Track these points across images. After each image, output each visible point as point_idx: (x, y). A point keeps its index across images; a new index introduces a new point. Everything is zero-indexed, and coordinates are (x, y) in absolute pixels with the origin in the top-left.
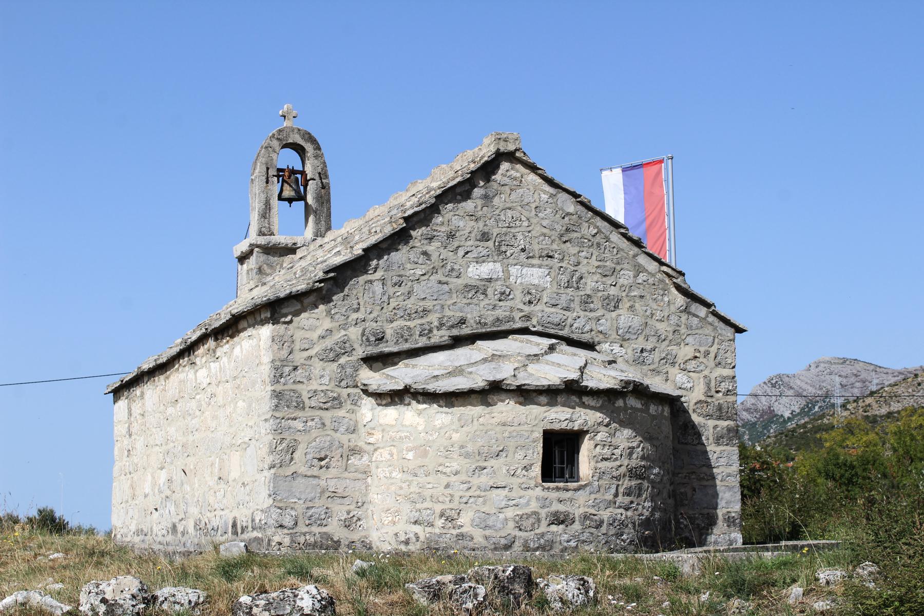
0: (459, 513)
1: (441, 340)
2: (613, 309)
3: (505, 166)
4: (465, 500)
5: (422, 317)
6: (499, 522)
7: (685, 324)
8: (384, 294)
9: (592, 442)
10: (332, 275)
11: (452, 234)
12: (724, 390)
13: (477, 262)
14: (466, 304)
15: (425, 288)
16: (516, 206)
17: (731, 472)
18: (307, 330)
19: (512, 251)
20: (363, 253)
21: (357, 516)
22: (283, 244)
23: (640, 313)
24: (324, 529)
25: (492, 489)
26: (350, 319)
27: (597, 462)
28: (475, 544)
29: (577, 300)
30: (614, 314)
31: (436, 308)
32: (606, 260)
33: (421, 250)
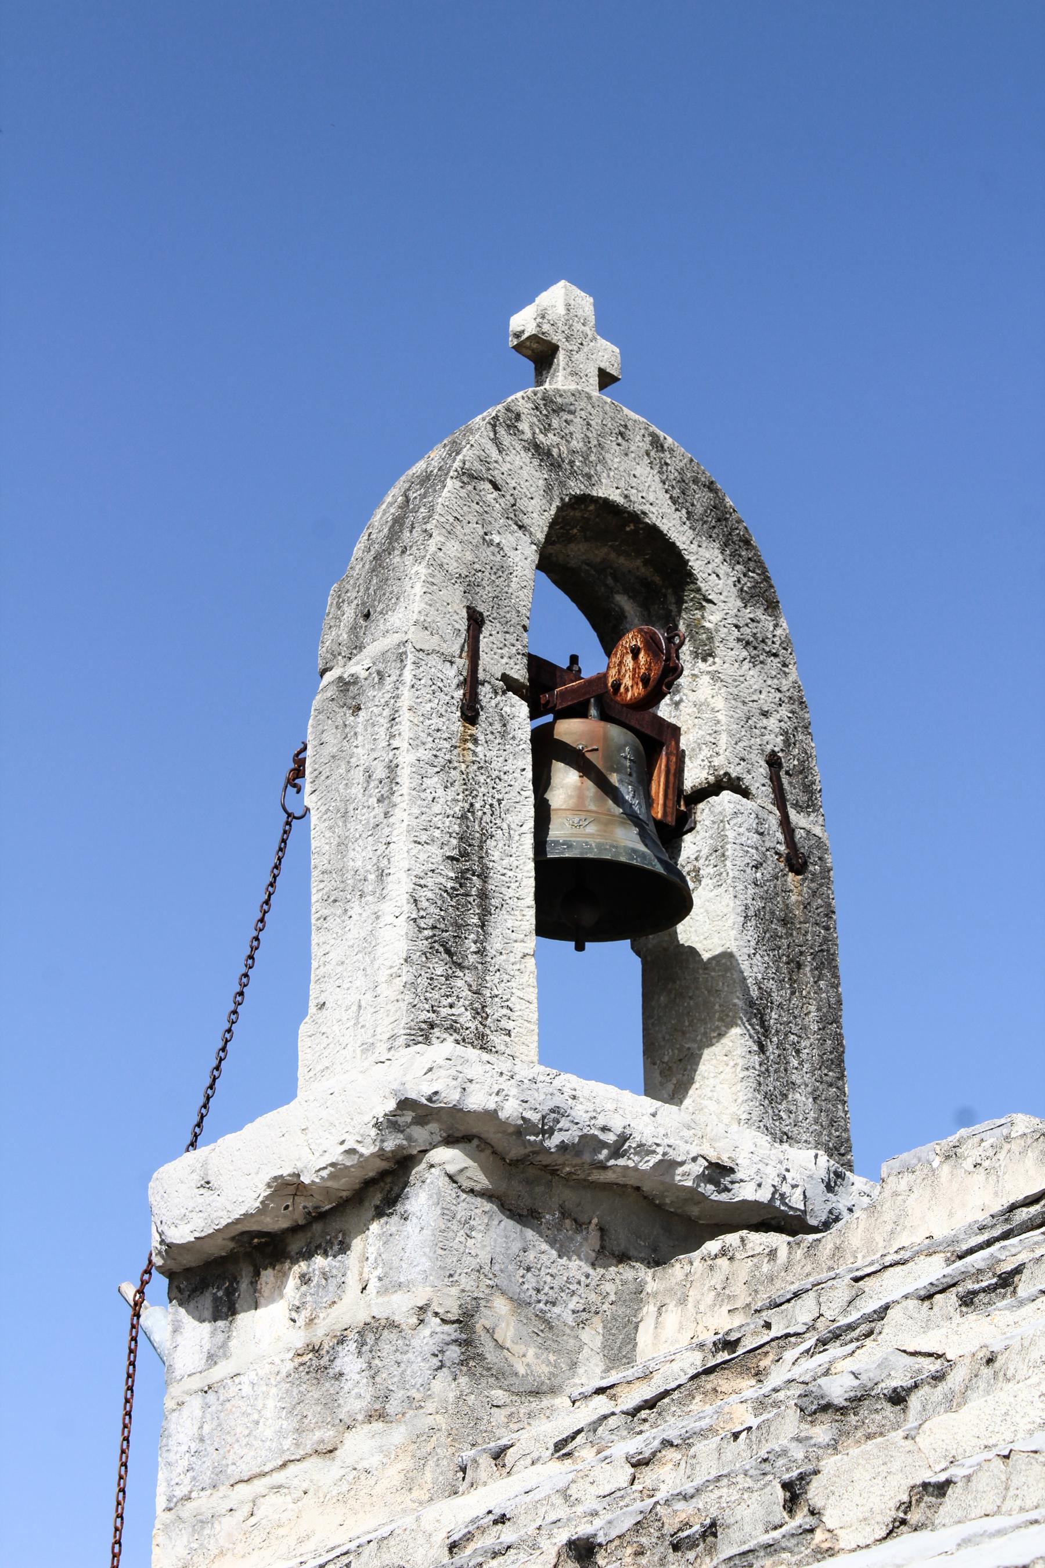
22: (643, 1150)
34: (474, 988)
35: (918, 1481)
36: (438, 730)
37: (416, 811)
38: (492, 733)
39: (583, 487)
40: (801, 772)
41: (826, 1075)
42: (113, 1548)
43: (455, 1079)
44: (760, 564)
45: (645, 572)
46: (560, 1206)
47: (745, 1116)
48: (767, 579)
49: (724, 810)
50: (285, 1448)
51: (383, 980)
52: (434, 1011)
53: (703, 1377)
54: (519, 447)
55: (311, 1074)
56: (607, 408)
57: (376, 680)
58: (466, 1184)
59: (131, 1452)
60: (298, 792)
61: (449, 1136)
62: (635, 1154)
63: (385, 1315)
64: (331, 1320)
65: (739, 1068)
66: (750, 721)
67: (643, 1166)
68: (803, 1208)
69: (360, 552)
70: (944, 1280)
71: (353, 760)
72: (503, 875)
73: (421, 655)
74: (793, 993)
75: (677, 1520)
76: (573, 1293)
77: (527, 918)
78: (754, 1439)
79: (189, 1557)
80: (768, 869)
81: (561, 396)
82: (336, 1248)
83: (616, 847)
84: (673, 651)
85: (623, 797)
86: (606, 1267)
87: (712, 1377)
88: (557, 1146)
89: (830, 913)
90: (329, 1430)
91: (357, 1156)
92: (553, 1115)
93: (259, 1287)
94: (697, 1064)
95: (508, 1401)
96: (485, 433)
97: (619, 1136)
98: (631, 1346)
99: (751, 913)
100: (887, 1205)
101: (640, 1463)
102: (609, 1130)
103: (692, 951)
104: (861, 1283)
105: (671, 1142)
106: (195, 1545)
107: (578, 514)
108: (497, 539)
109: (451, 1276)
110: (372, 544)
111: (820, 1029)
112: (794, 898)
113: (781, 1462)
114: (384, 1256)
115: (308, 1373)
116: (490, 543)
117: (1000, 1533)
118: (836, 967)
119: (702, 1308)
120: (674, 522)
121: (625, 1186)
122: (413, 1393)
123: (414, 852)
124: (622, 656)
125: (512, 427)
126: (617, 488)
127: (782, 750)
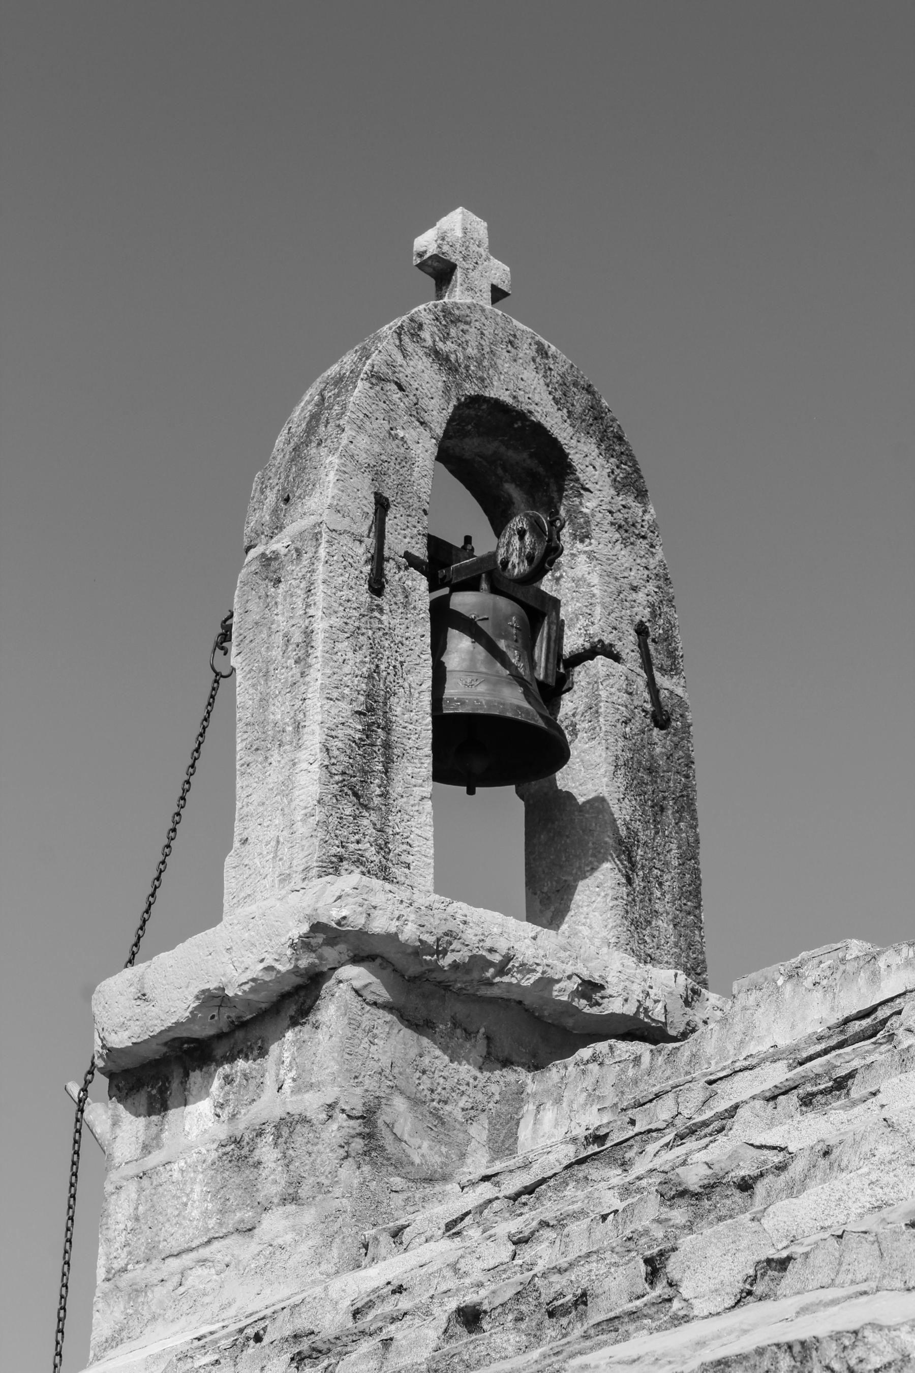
22: (525, 969)
34: (378, 826)
35: (763, 1258)
36: (348, 601)
37: (329, 671)
38: (396, 603)
39: (477, 389)
40: (665, 640)
41: (685, 904)
42: (59, 1313)
43: (361, 905)
44: (631, 457)
45: (532, 463)
46: (452, 1017)
47: (613, 940)
48: (637, 471)
49: (598, 672)
50: (210, 1227)
51: (299, 818)
52: (343, 847)
53: (576, 1167)
54: (421, 353)
55: (235, 900)
56: (498, 319)
57: (295, 556)
58: (370, 998)
59: (75, 1230)
60: (225, 654)
61: (355, 956)
62: (518, 972)
63: (298, 1112)
64: (251, 1116)
65: (609, 898)
66: (621, 595)
67: (525, 983)
68: (663, 1020)
69: (281, 446)
70: (787, 1084)
71: (274, 626)
72: (405, 728)
73: (334, 535)
74: (657, 833)
75: (552, 1290)
76: (463, 1093)
77: (426, 765)
78: (620, 1220)
79: (125, 1321)
80: (636, 724)
81: (458, 308)
82: (256, 1052)
83: (503, 704)
84: (554, 533)
85: (510, 661)
86: (491, 1070)
87: (584, 1166)
88: (449, 965)
89: (690, 763)
90: (248, 1211)
91: (275, 973)
92: (447, 938)
93: (188, 1086)
94: (573, 894)
95: (405, 1187)
96: (392, 341)
97: (504, 956)
98: (512, 1140)
99: (621, 763)
100: (736, 1019)
101: (520, 1241)
102: (496, 951)
103: (569, 796)
104: (714, 1085)
105: (550, 961)
106: (130, 1311)
107: (472, 412)
108: (401, 433)
109: (356, 1077)
110: (291, 437)
111: (680, 865)
112: (658, 750)
113: (643, 1240)
114: (297, 1060)
115: (230, 1161)
116: (395, 437)
117: (834, 1302)
118: (694, 810)
119: (575, 1107)
120: (556, 420)
121: (509, 1000)
122: (322, 1179)
123: (326, 707)
124: (510, 537)
125: (415, 336)
126: (507, 390)
127: (649, 621)
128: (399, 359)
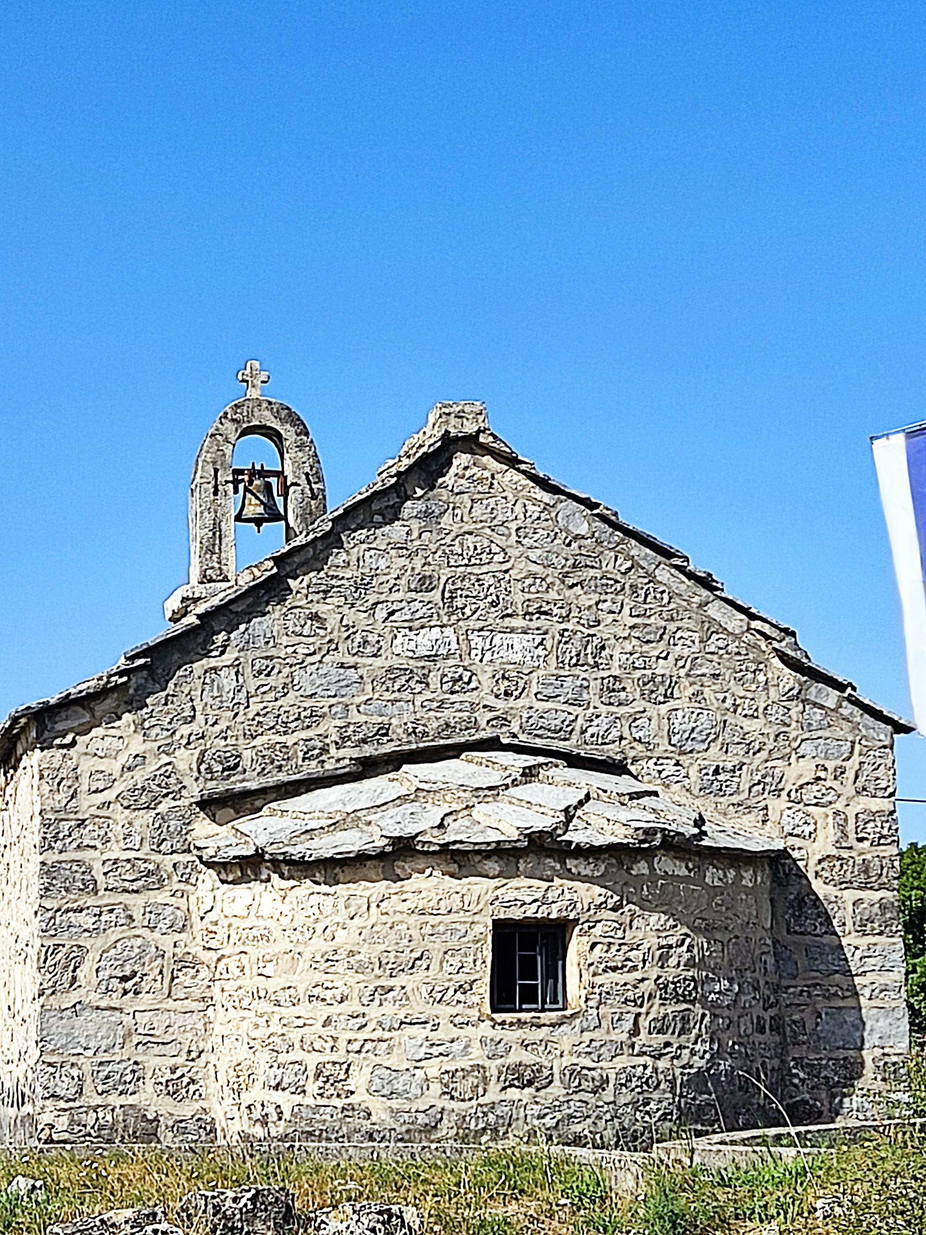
0: (347, 1070)
1: (338, 766)
2: (661, 699)
3: (461, 459)
4: (356, 1046)
5: (308, 727)
6: (414, 1085)
7: (797, 722)
8: (239, 691)
9: (586, 939)
10: (142, 661)
11: (365, 582)
12: (872, 836)
13: (410, 629)
14: (388, 701)
15: (314, 676)
16: (483, 528)
17: (888, 982)
18: (101, 758)
19: (474, 607)
20: (198, 622)
21: (190, 1075)
23: (712, 704)
24: (131, 1100)
25: (403, 1026)
26: (177, 736)
27: (594, 975)
28: (374, 1124)
29: (595, 686)
30: (664, 709)
31: (334, 710)
32: (648, 614)
33: (307, 612)
125: (226, 417)
128: (220, 426)
